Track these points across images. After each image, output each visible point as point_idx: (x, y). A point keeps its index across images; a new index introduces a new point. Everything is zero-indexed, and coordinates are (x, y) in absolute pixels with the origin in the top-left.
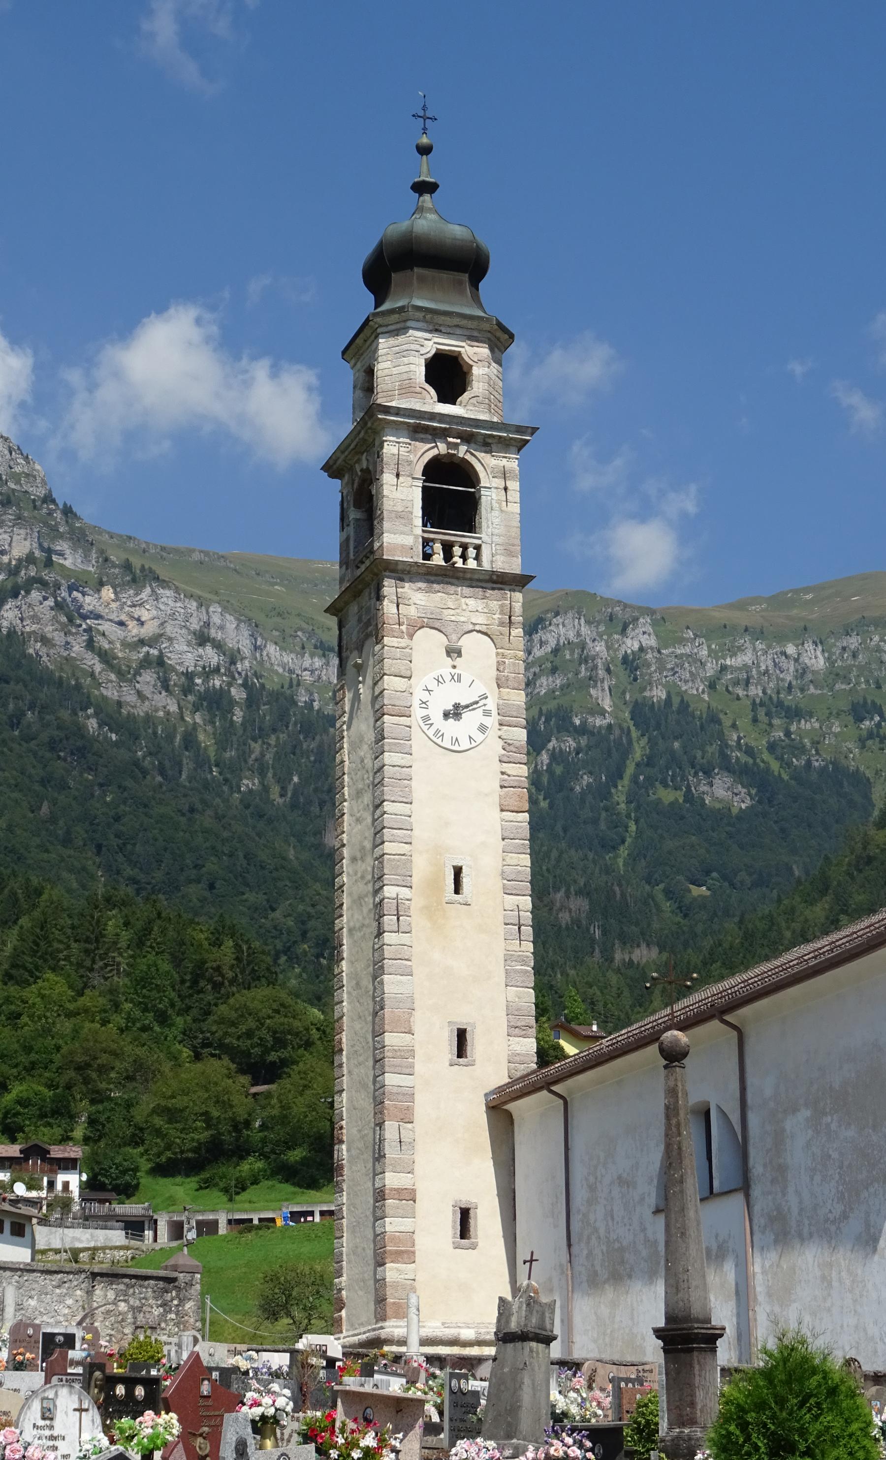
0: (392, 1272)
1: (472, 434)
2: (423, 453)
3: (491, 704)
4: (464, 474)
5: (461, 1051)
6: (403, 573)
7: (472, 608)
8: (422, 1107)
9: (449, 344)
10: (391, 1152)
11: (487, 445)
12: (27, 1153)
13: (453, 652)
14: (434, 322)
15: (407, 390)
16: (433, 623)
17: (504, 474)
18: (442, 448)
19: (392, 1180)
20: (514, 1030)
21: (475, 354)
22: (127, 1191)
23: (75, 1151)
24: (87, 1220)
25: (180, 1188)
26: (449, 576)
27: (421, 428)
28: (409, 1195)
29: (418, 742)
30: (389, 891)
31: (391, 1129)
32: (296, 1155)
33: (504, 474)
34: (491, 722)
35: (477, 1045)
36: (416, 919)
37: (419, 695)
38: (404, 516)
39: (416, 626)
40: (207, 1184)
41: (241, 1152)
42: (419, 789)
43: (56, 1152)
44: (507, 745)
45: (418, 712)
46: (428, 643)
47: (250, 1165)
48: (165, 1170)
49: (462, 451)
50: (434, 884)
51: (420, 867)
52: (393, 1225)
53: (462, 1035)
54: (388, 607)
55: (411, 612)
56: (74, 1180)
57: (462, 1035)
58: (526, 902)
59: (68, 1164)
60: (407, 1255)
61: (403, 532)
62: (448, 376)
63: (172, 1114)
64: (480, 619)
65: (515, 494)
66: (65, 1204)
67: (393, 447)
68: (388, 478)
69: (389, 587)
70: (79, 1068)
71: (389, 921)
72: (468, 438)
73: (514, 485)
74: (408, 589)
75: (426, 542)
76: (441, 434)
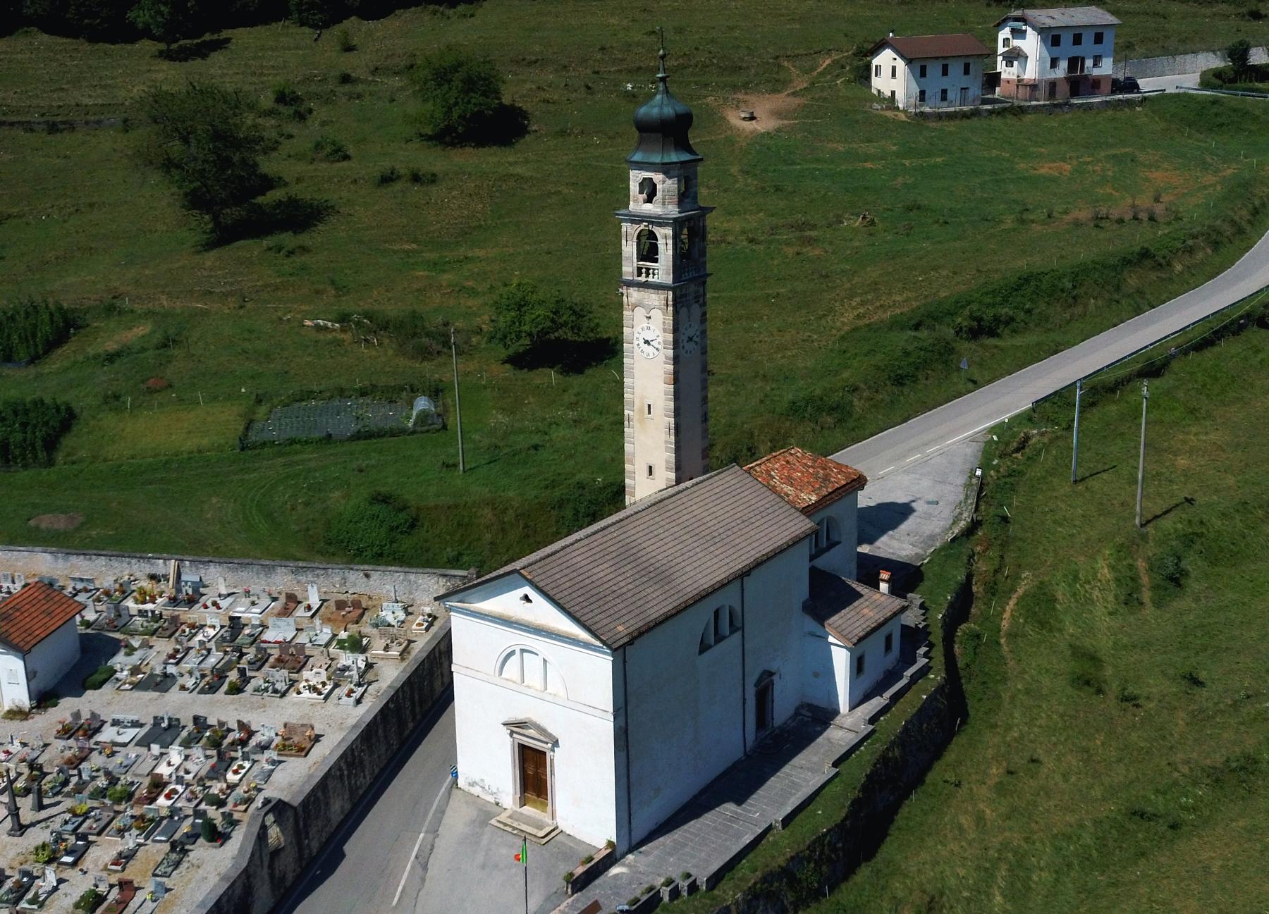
3: (660, 339)
4: (652, 236)
5: (651, 473)
6: (630, 284)
7: (656, 299)
11: (660, 225)
14: (640, 166)
18: (642, 227)
21: (657, 177)
26: (646, 285)
27: (636, 219)
36: (635, 423)
37: (636, 335)
45: (636, 342)
46: (640, 312)
53: (650, 468)
55: (632, 300)
57: (650, 468)
62: (650, 191)
64: (656, 303)
65: (670, 246)
67: (626, 227)
68: (624, 242)
72: (650, 222)
73: (670, 242)
74: (631, 290)
76: (641, 222)
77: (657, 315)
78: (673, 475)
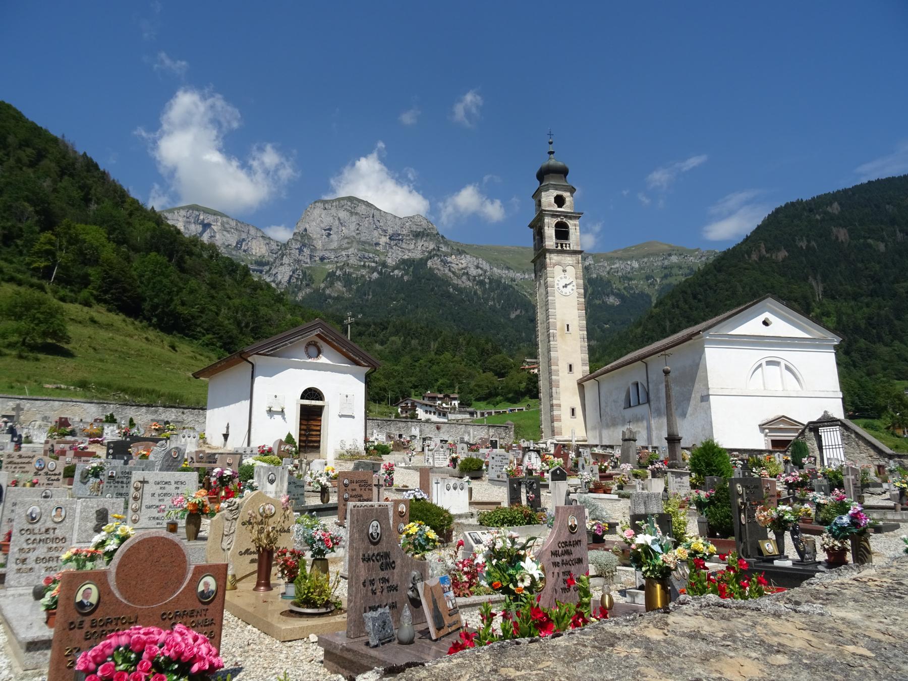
0: (556, 424)
1: (567, 215)
2: (555, 221)
3: (574, 283)
6: (551, 251)
7: (569, 259)
8: (561, 384)
9: (560, 193)
10: (554, 395)
11: (570, 218)
12: (445, 396)
13: (564, 271)
14: (556, 187)
15: (550, 205)
16: (559, 264)
17: (575, 225)
18: (559, 220)
19: (555, 402)
20: (583, 364)
21: (566, 195)
22: (469, 405)
23: (456, 396)
24: (460, 412)
25: (482, 404)
26: (562, 252)
27: (554, 215)
28: (559, 406)
29: (557, 294)
30: (551, 331)
31: (554, 389)
32: (510, 395)
33: (575, 225)
34: (575, 288)
35: (574, 368)
36: (558, 338)
37: (556, 282)
38: (551, 237)
39: (555, 265)
40: (488, 403)
41: (497, 395)
42: (557, 305)
43: (452, 396)
44: (579, 294)
45: (556, 286)
46: (558, 269)
47: (499, 398)
48: (478, 400)
49: (564, 220)
50: (562, 329)
51: (559, 325)
52: (555, 413)
53: (570, 366)
54: (548, 260)
56: (456, 403)
57: (570, 366)
58: (585, 333)
59: (455, 399)
60: (559, 420)
61: (550, 240)
62: (560, 201)
63: (479, 386)
65: (578, 230)
66: (454, 408)
67: (547, 220)
68: (546, 228)
69: (548, 255)
70: (455, 375)
71: (551, 338)
72: (566, 217)
73: (578, 228)
74: (552, 255)
75: (557, 244)
76: (558, 216)
77: (571, 270)
78: (587, 368)
